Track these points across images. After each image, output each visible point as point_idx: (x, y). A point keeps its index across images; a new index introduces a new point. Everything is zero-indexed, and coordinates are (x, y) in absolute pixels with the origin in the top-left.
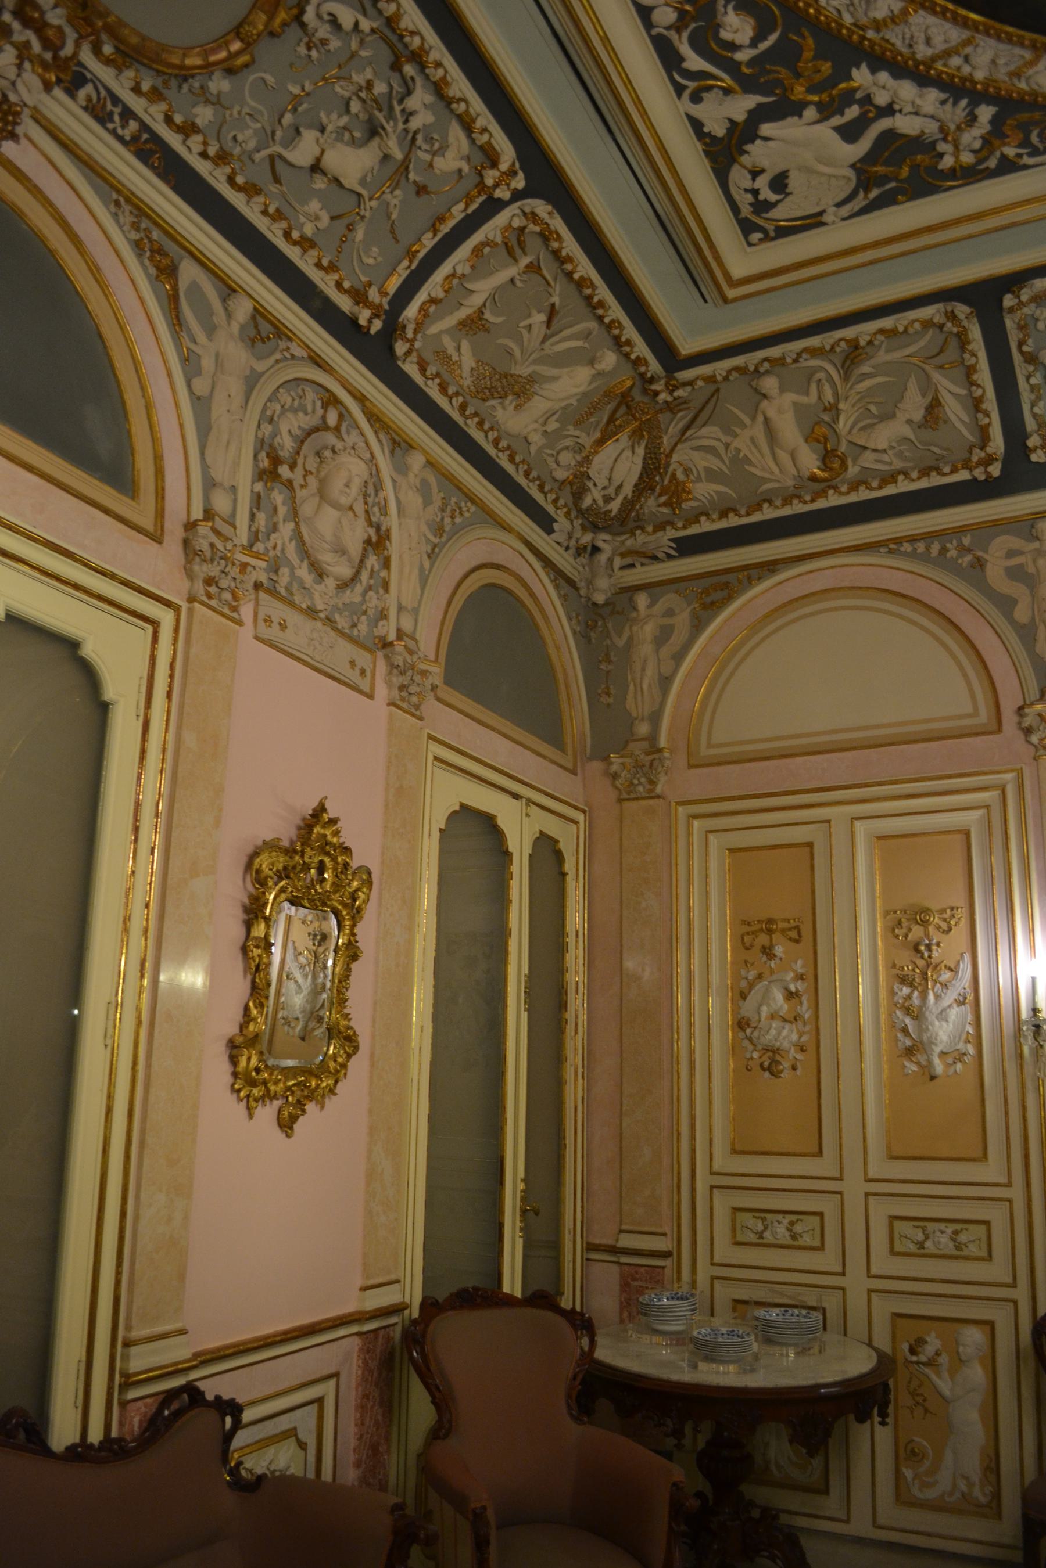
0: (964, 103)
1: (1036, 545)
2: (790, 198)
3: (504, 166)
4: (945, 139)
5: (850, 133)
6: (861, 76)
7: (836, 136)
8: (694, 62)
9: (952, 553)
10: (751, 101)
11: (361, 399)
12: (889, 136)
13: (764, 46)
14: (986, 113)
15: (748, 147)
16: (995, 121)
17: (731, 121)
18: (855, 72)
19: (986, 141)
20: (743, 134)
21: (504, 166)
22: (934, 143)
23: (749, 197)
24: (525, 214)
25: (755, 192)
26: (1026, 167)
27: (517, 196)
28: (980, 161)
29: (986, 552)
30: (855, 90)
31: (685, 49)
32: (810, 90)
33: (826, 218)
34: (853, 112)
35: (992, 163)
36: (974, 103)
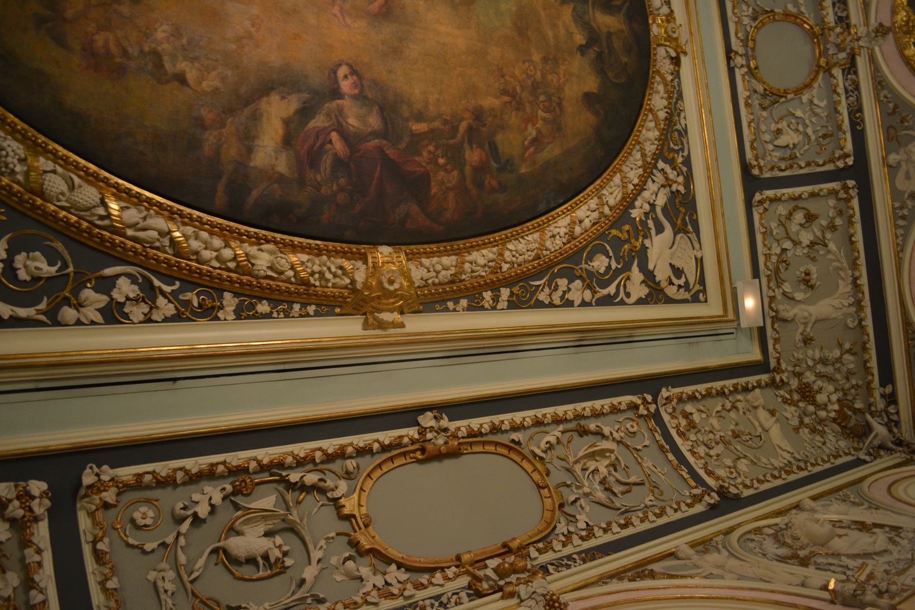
0: (654, 171)
1: (903, 165)
2: (685, 270)
3: (639, 402)
4: (670, 186)
5: (660, 229)
6: (636, 213)
7: (660, 236)
8: (611, 289)
9: (905, 212)
10: (635, 268)
11: (758, 519)
12: (664, 209)
13: (611, 254)
14: (661, 165)
15: (657, 279)
16: (666, 161)
17: (642, 282)
18: (633, 216)
19: (674, 169)
20: (649, 277)
21: (639, 402)
22: (672, 192)
23: (682, 290)
24: (665, 404)
25: (680, 286)
26: (689, 155)
27: (655, 401)
28: (683, 174)
29: (905, 192)
30: (641, 219)
31: (605, 292)
32: (637, 240)
33: (699, 255)
34: (651, 223)
35: (684, 169)
36: (655, 167)
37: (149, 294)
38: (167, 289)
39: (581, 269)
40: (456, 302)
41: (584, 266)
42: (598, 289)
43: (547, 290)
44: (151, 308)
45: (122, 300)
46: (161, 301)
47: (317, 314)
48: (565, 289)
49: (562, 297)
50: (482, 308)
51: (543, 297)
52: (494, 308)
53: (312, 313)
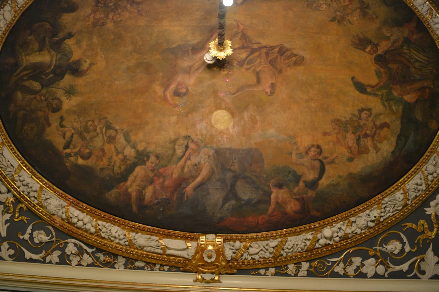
8: (405, 267)
13: (405, 240)
31: (398, 268)
37: (81, 252)
38: (90, 250)
39: (376, 250)
40: (267, 269)
41: (378, 248)
42: (391, 265)
43: (342, 265)
44: (81, 259)
45: (69, 254)
46: (86, 256)
47: (169, 270)
48: (359, 264)
49: (356, 271)
50: (287, 275)
51: (339, 269)
52: (296, 275)
53: (166, 270)
